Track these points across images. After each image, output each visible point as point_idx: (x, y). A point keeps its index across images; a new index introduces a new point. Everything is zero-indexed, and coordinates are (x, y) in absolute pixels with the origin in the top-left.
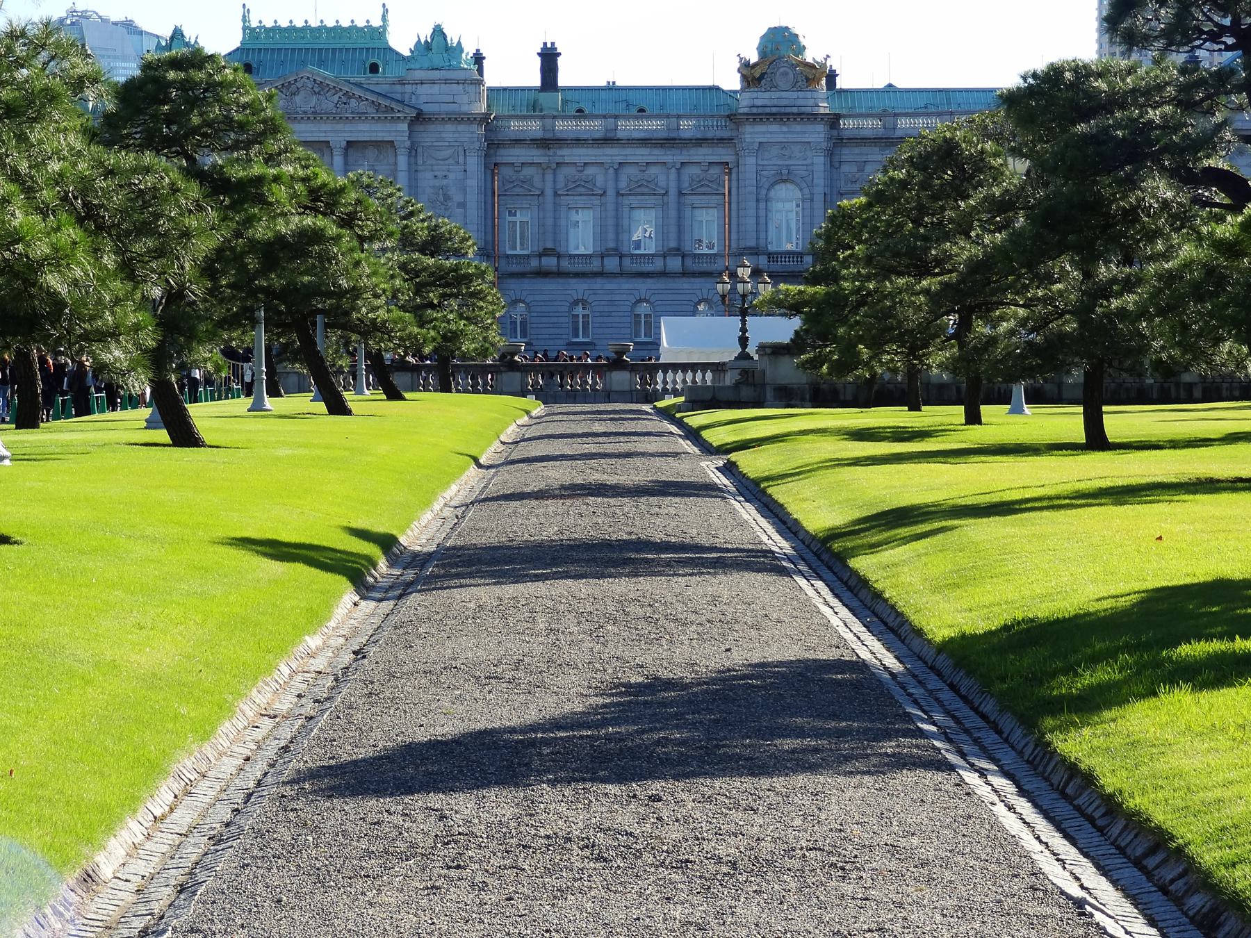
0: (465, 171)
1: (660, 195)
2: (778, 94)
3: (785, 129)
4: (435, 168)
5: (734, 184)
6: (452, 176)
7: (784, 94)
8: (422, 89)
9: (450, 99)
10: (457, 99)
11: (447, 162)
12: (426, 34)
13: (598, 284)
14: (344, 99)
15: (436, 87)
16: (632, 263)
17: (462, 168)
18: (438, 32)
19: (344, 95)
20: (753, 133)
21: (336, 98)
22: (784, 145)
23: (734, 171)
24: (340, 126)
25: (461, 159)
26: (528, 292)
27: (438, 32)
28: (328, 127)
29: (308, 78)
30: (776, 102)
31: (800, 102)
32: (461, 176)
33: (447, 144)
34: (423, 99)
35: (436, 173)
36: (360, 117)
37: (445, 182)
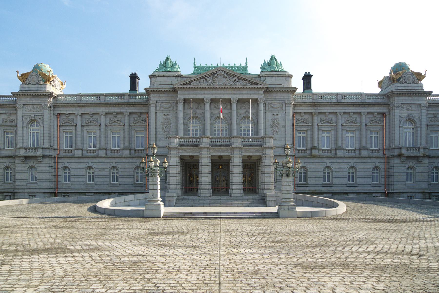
0: (286, 113)
1: (358, 126)
2: (407, 85)
3: (410, 98)
4: (273, 111)
5: (387, 121)
6: (280, 115)
7: (409, 85)
8: (268, 79)
9: (279, 83)
10: (282, 83)
11: (278, 109)
12: (268, 59)
13: (334, 161)
14: (237, 80)
15: (274, 78)
16: (347, 152)
17: (284, 111)
18: (273, 58)
19: (237, 78)
20: (398, 100)
21: (234, 79)
22: (410, 105)
23: (388, 116)
24: (235, 92)
25: (284, 108)
26: (307, 163)
27: (273, 58)
28: (230, 92)
29: (222, 71)
30: (406, 88)
31: (416, 88)
32: (284, 114)
33: (278, 101)
34: (268, 83)
35: (274, 114)
36: (244, 88)
37: (276, 117)
